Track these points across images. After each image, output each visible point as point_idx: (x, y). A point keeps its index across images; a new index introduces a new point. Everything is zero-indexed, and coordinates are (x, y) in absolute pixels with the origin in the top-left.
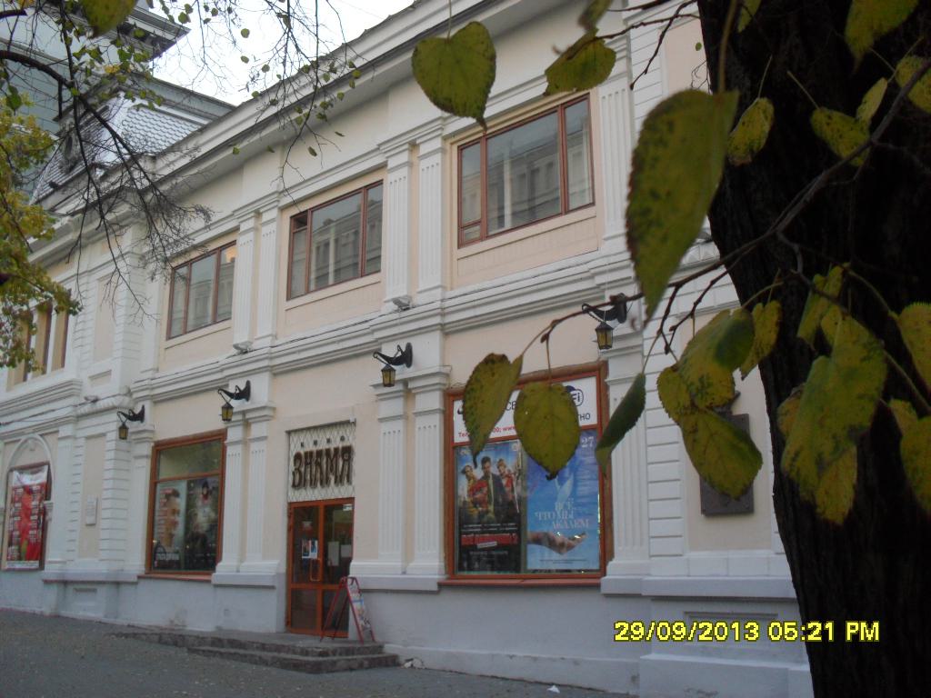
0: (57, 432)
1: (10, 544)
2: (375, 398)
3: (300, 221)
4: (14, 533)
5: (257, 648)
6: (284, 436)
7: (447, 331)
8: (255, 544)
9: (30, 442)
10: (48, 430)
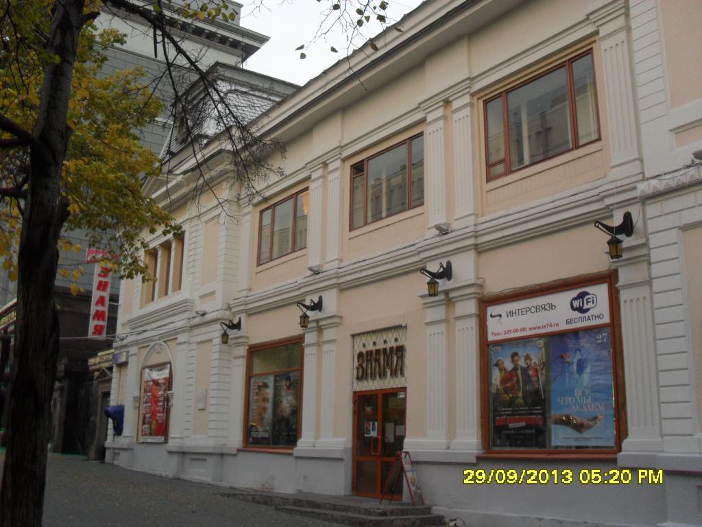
0: (176, 338)
1: (144, 423)
2: (422, 306)
3: (358, 169)
4: (147, 415)
5: (330, 508)
6: (350, 338)
7: (480, 250)
8: (327, 425)
9: (157, 346)
10: (170, 337)
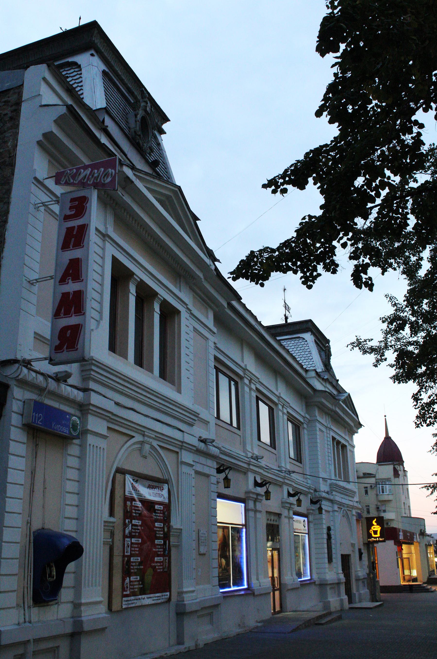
4: (132, 559)
